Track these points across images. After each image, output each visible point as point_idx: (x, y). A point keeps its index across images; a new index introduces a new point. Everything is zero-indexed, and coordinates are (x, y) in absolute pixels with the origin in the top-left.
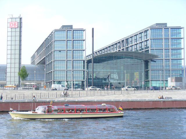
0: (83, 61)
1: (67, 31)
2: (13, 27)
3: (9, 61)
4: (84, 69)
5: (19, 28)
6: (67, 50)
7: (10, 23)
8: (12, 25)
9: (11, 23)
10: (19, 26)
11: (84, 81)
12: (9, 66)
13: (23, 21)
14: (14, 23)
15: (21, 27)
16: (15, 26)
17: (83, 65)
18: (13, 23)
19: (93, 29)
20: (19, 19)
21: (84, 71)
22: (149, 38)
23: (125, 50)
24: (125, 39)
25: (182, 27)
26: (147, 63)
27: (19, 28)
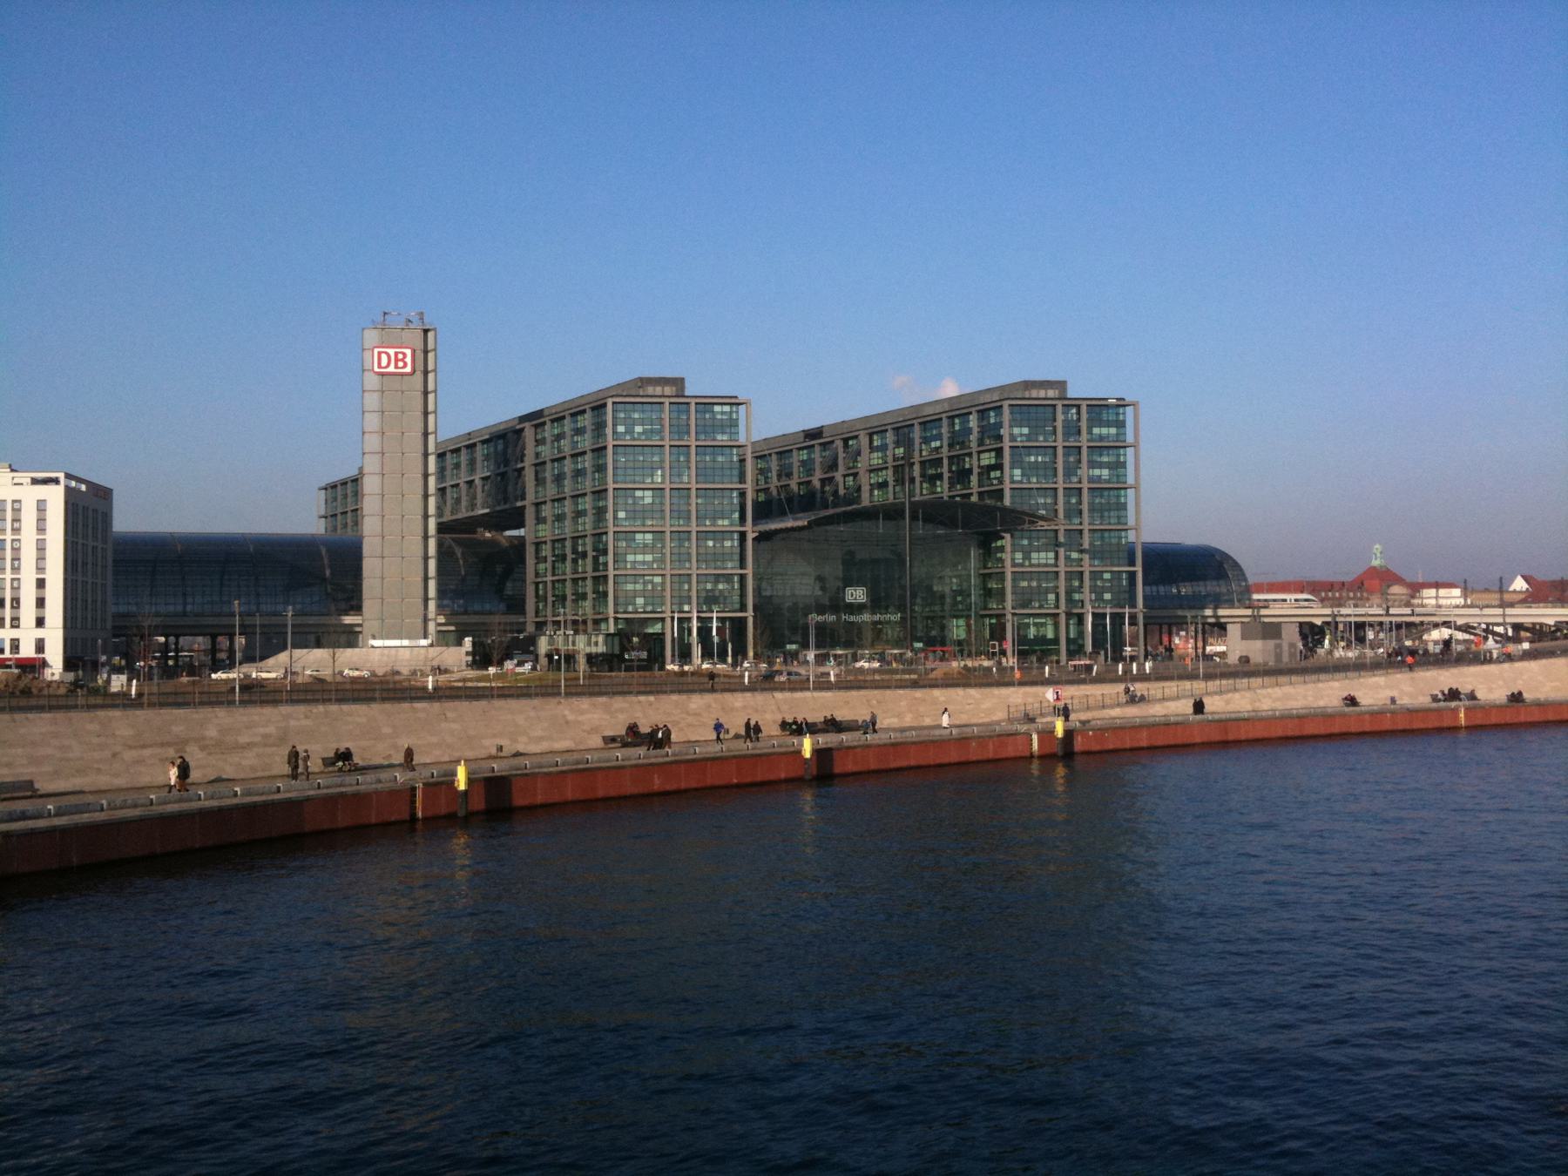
0: (736, 536)
2: (392, 369)
4: (742, 565)
9: (380, 353)
10: (420, 366)
11: (746, 618)
14: (396, 354)
15: (426, 373)
16: (401, 364)
21: (742, 578)
25: (1129, 399)
27: (419, 376)
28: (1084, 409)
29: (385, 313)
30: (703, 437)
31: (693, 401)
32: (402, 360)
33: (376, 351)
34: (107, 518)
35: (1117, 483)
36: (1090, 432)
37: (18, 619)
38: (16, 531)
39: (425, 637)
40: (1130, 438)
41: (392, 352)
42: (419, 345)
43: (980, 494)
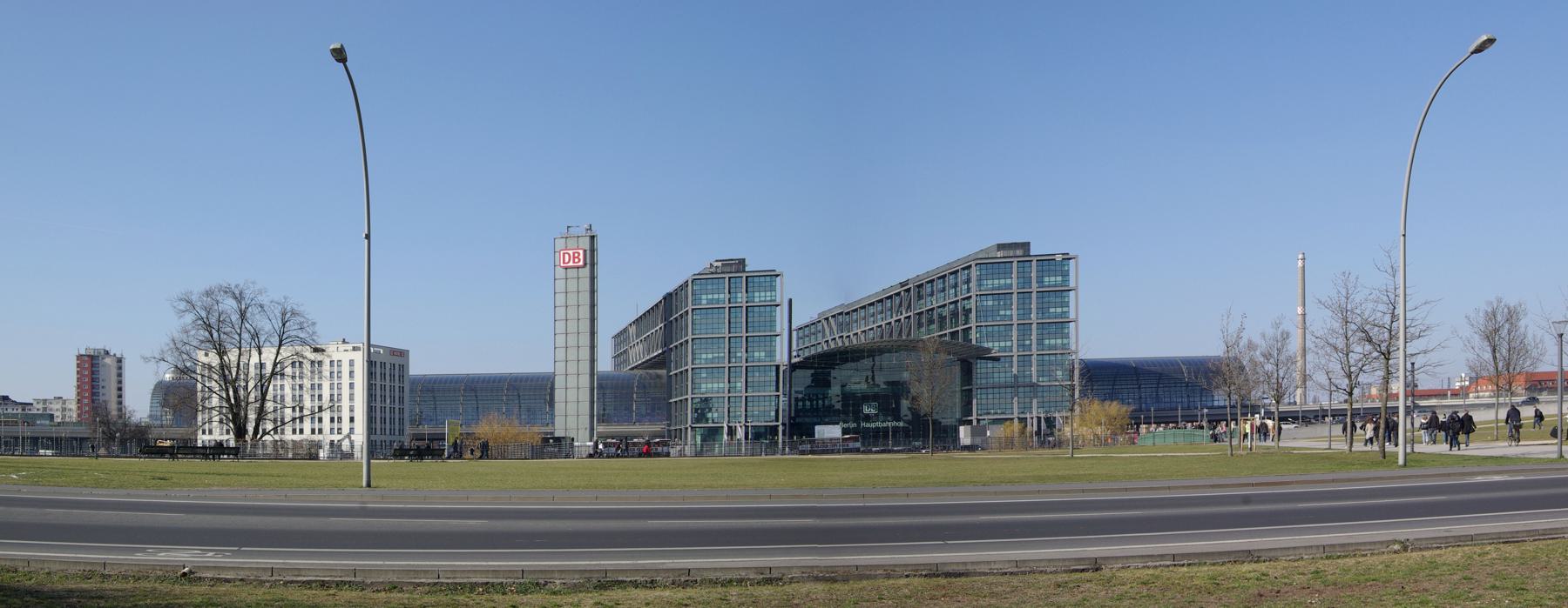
0: (774, 368)
1: (730, 278)
2: (571, 264)
5: (588, 266)
6: (731, 335)
8: (567, 260)
9: (564, 254)
10: (588, 261)
12: (559, 382)
14: (574, 253)
15: (593, 265)
17: (774, 378)
18: (571, 252)
20: (588, 239)
22: (972, 293)
23: (886, 338)
29: (568, 227)
32: (578, 257)
33: (562, 252)
34: (403, 368)
35: (993, 321)
36: (1040, 281)
37: (341, 429)
38: (339, 377)
39: (591, 441)
40: (1072, 284)
41: (571, 252)
42: (587, 247)
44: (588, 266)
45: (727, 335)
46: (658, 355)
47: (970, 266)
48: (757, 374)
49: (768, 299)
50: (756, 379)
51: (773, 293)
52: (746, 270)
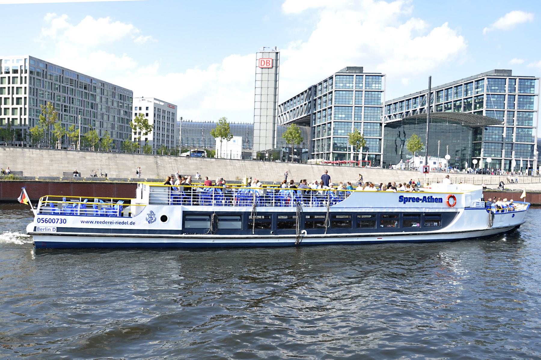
0: (379, 124)
2: (265, 66)
3: (257, 119)
7: (260, 60)
8: (263, 64)
10: (274, 65)
12: (256, 126)
13: (281, 56)
14: (267, 61)
15: (276, 67)
16: (268, 64)
18: (265, 60)
19: (430, 78)
20: (275, 54)
24: (434, 91)
26: (477, 131)
27: (274, 68)
28: (517, 80)
30: (368, 88)
31: (365, 75)
33: (260, 60)
42: (274, 58)
43: (474, 112)
44: (274, 68)
45: (354, 105)
46: (305, 117)
47: (484, 79)
48: (369, 127)
49: (377, 88)
50: (369, 130)
51: (380, 85)
52: (364, 72)
